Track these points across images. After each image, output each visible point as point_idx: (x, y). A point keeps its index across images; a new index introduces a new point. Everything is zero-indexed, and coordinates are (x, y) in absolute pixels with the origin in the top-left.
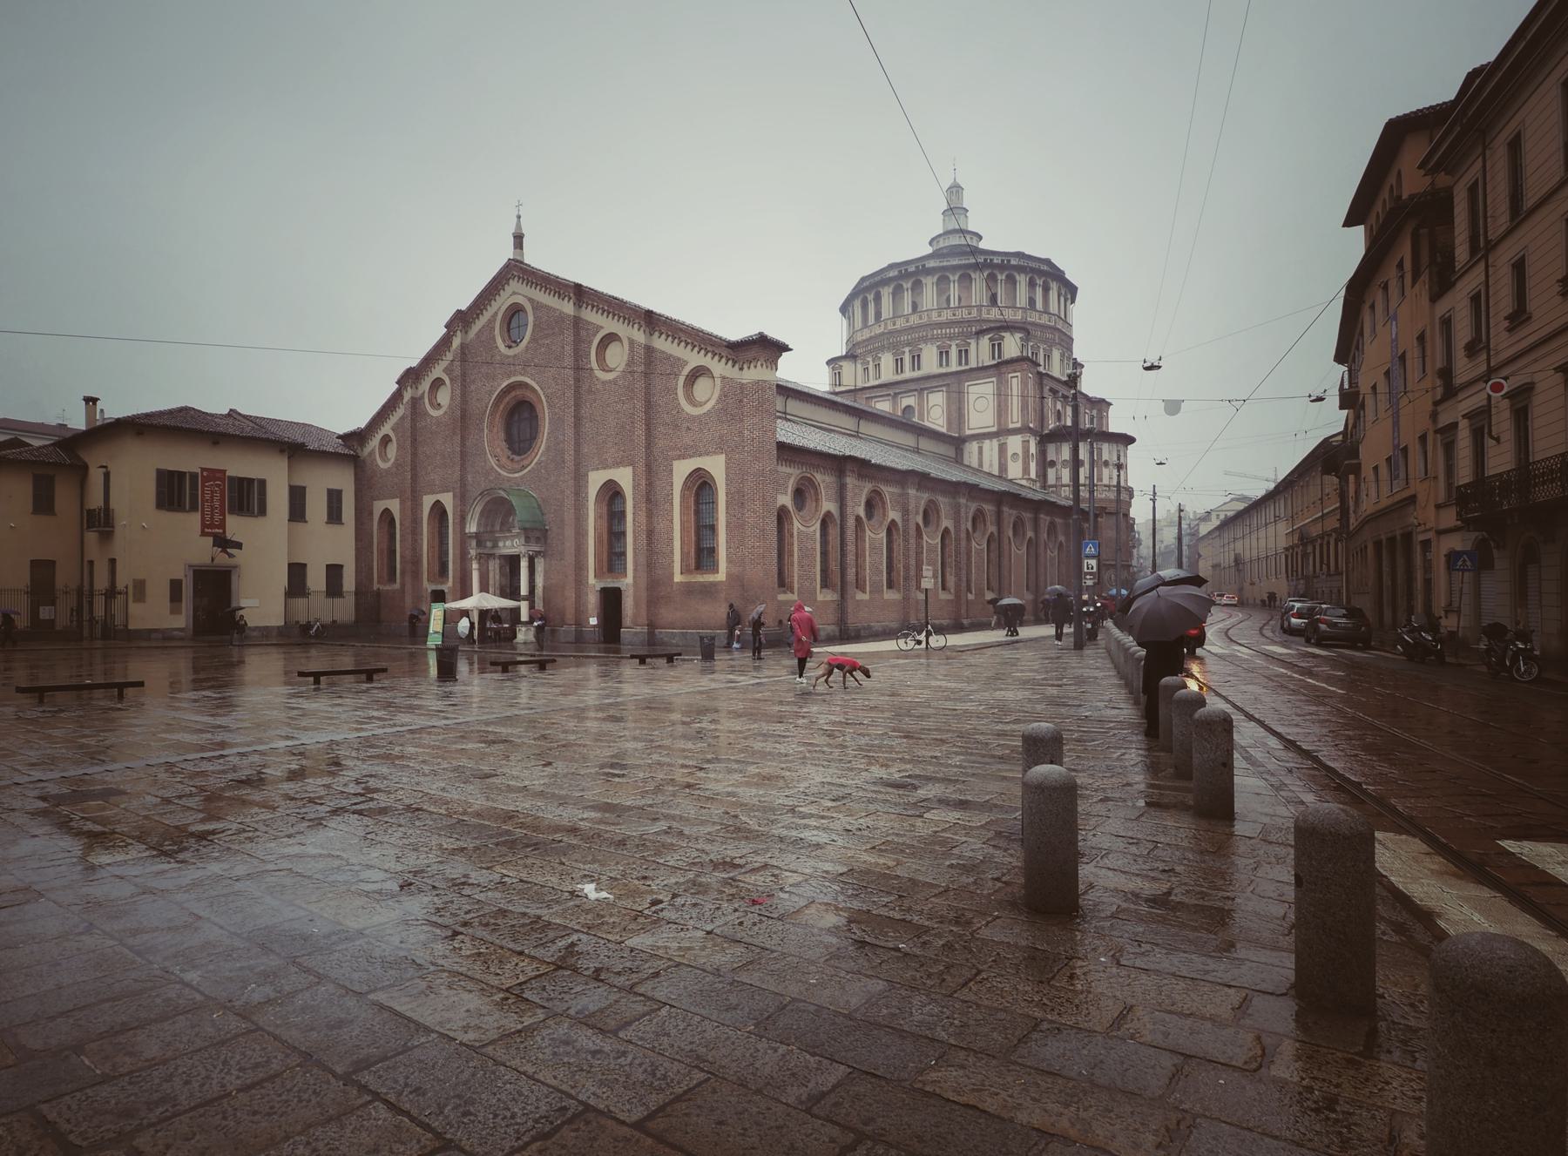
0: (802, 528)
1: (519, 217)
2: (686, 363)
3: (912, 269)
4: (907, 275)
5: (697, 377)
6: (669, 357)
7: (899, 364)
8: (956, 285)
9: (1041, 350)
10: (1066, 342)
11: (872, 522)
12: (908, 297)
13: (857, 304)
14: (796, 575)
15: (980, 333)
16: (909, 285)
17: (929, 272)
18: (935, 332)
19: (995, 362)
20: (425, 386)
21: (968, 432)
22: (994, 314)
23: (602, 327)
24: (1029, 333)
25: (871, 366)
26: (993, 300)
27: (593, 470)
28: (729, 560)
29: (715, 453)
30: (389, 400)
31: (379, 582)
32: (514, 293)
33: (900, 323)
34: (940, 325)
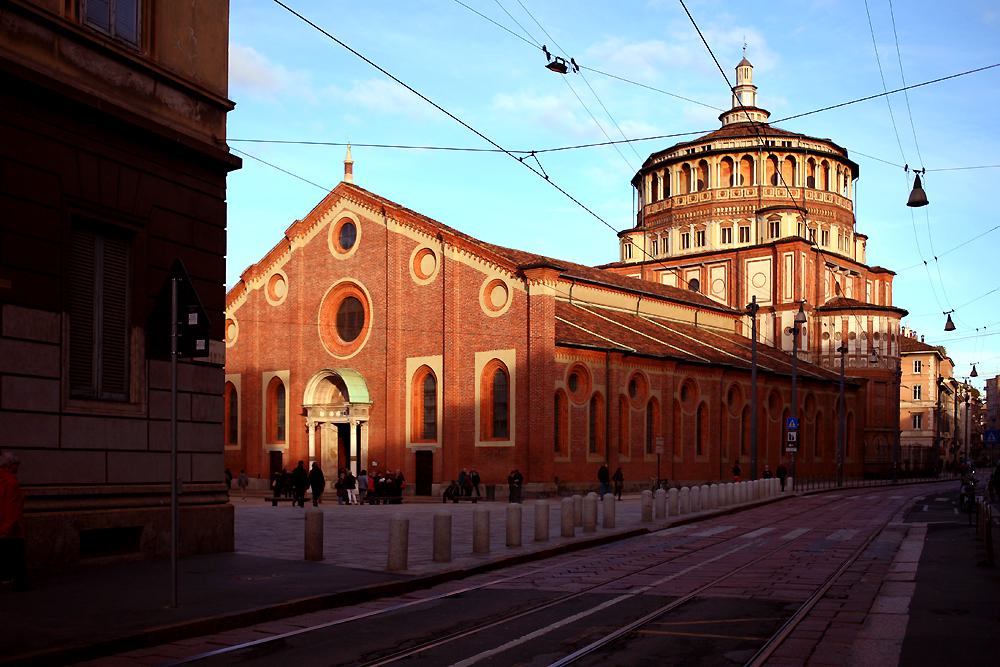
0: (575, 405)
2: (486, 276)
3: (698, 149)
4: (693, 156)
6: (470, 271)
7: (686, 243)
9: (819, 227)
10: (847, 218)
11: (634, 399)
12: (695, 177)
13: (649, 180)
14: (569, 442)
15: (760, 213)
17: (717, 153)
19: (770, 241)
20: (265, 279)
22: (772, 195)
27: (410, 357)
28: (518, 431)
29: (509, 348)
32: (345, 209)
33: (687, 201)
34: (722, 204)
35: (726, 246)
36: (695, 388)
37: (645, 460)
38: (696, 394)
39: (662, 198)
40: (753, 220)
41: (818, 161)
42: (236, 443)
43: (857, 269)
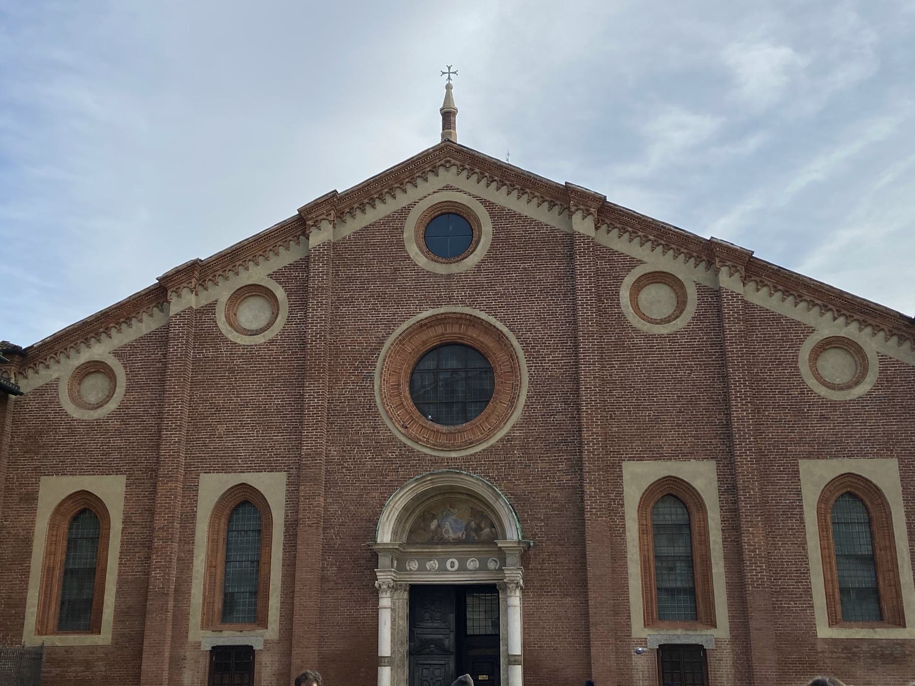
1: (449, 87)
5: (825, 350)
6: (777, 318)
20: (221, 292)
23: (641, 262)
27: (631, 459)
29: (878, 455)
30: (120, 306)
31: (41, 630)
42: (95, 628)
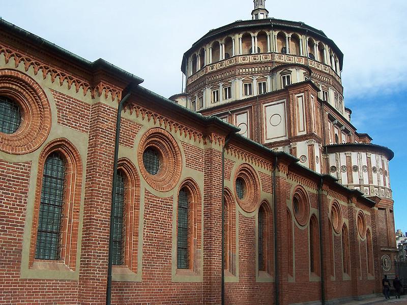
7: (216, 94)
8: (256, 39)
12: (222, 50)
15: (273, 72)
16: (223, 41)
18: (241, 70)
21: (266, 142)
22: (284, 59)
24: (310, 72)
25: (196, 102)
26: (284, 51)
33: (217, 67)
35: (248, 97)
36: (175, 154)
37: (26, 272)
38: (176, 163)
39: (199, 69)
40: (269, 80)
41: (316, 42)
43: (349, 128)
